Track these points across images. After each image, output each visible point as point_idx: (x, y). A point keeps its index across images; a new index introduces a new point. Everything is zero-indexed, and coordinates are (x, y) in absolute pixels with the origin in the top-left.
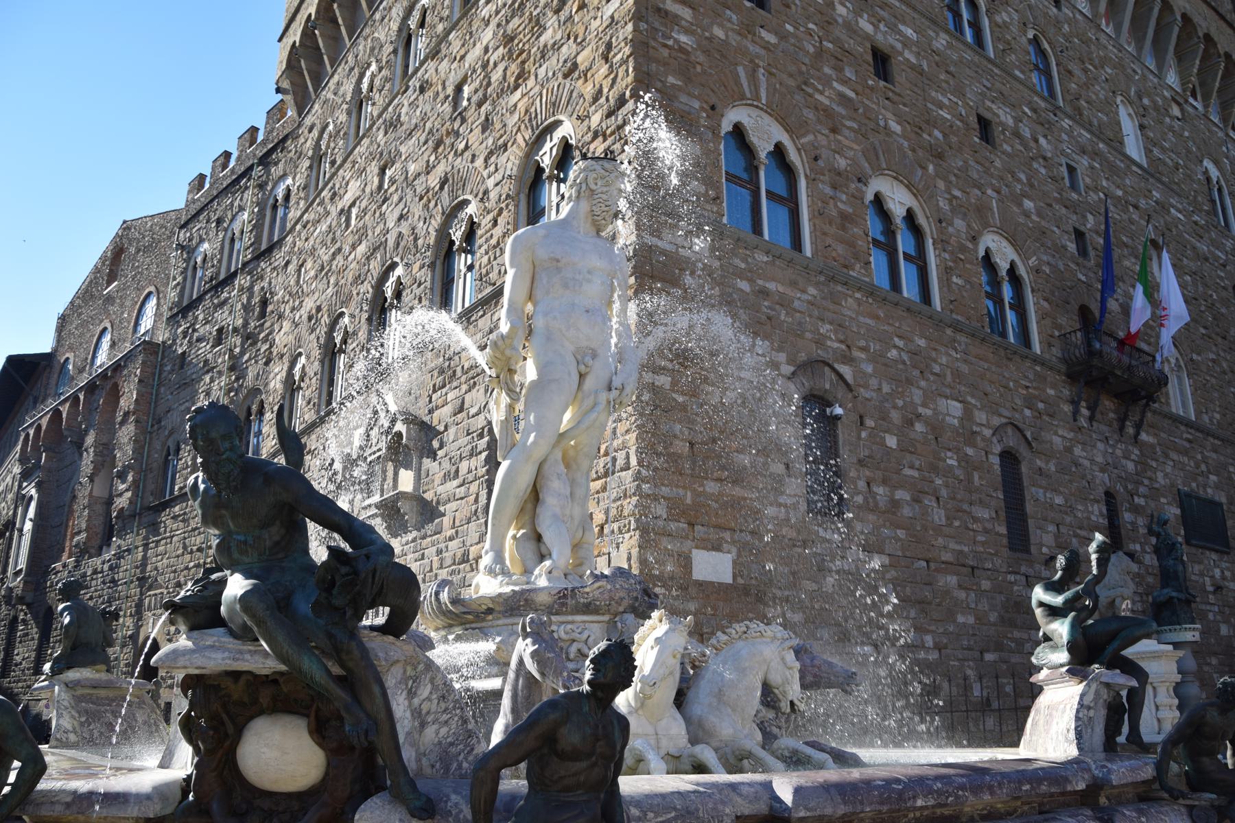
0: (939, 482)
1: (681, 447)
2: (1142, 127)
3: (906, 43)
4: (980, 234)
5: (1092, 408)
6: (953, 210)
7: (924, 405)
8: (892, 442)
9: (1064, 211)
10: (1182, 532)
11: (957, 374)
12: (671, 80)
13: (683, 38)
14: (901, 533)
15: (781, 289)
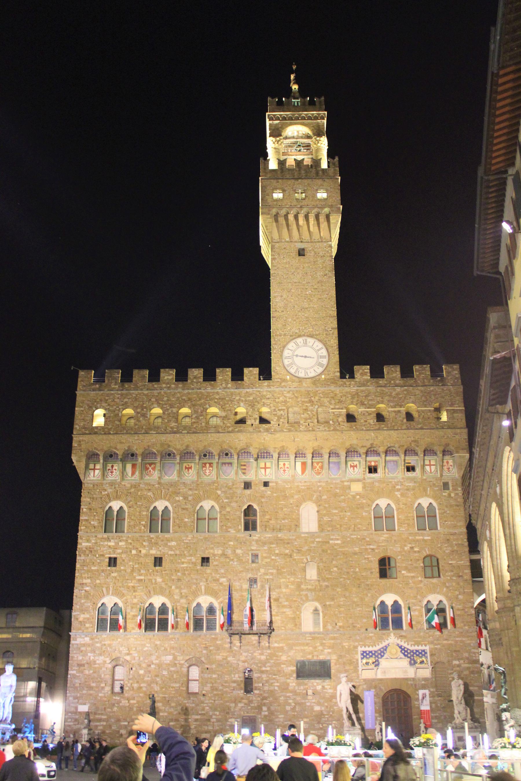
0: (158, 679)
1: (77, 685)
2: (318, 512)
3: (171, 548)
4: (194, 600)
5: (241, 643)
6: (182, 597)
7: (156, 660)
8: (142, 672)
9: (244, 574)
10: (295, 675)
11: (173, 648)
12: (83, 601)
13: (87, 588)
14: (141, 695)
15: (109, 642)
